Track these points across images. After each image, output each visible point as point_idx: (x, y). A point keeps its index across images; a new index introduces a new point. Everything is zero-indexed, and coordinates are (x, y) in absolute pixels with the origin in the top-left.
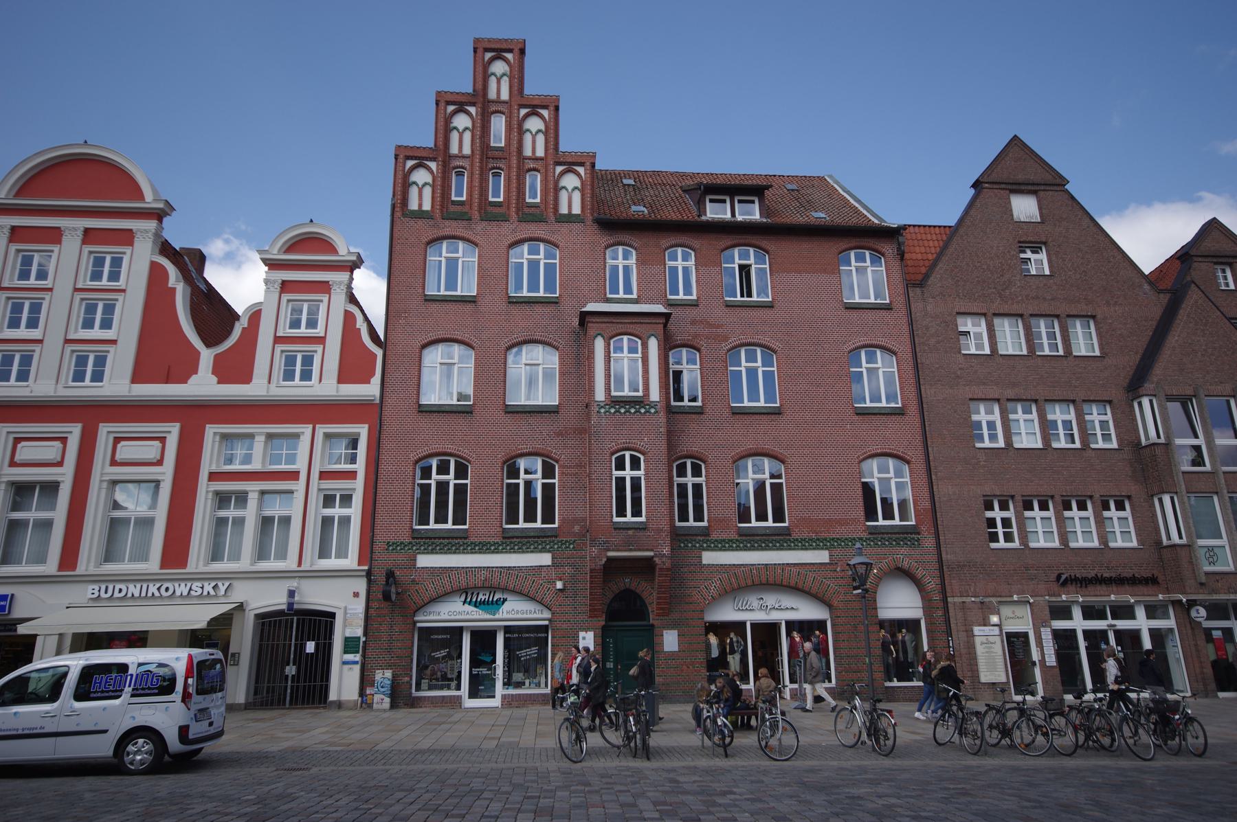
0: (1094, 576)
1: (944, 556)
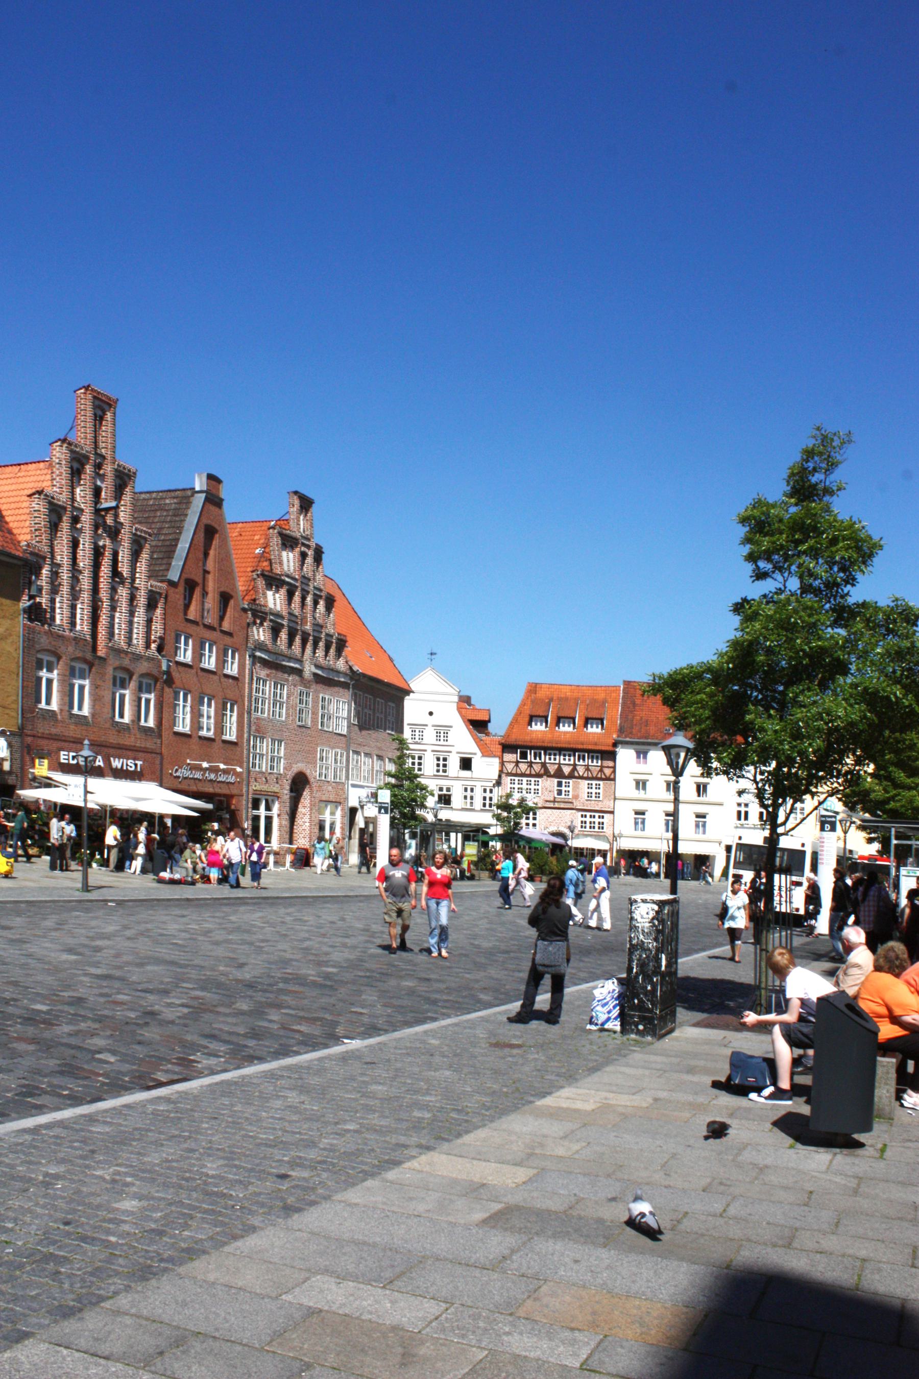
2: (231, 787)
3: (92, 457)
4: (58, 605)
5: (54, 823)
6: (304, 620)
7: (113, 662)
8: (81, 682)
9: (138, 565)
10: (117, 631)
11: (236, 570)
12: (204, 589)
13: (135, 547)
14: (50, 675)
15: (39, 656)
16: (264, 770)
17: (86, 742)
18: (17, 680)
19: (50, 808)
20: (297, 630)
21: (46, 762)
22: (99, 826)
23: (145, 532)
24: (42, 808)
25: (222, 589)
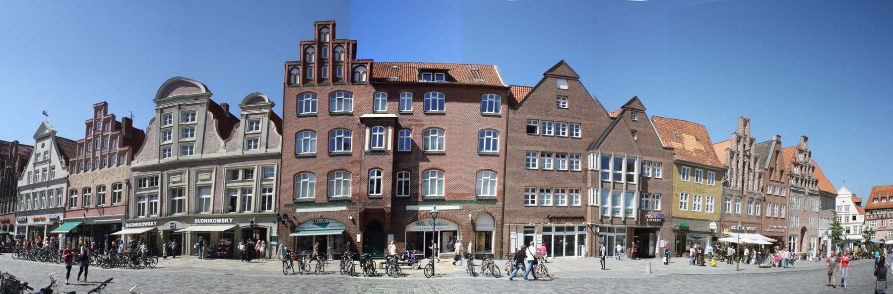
4: (732, 181)
5: (729, 249)
7: (748, 196)
8: (738, 203)
14: (729, 202)
21: (727, 229)
22: (742, 249)
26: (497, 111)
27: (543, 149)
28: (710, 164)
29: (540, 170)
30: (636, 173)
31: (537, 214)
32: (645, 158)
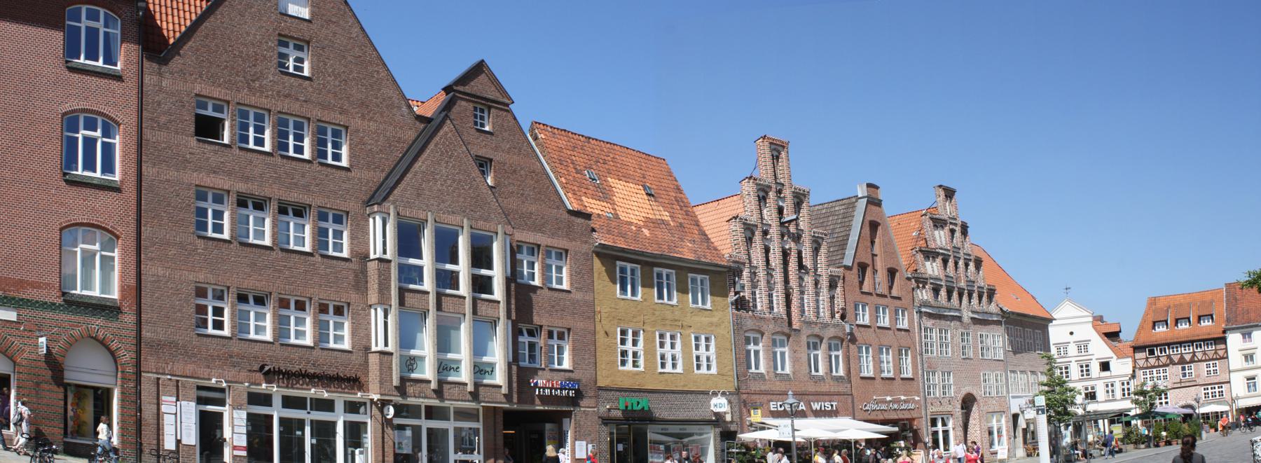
0: (299, 370)
1: (144, 333)
2: (912, 412)
3: (774, 186)
4: (758, 296)
6: (958, 279)
7: (806, 331)
9: (819, 258)
10: (806, 309)
11: (898, 250)
12: (874, 268)
13: (815, 245)
14: (756, 348)
15: (747, 335)
16: (938, 395)
17: (790, 393)
18: (732, 355)
19: (765, 445)
20: (954, 288)
21: (759, 411)
22: (806, 454)
23: (822, 233)
24: (759, 445)
25: (889, 266)
26: (109, 60)
27: (242, 187)
28: (691, 256)
29: (235, 243)
30: (497, 273)
31: (231, 357)
32: (520, 236)
